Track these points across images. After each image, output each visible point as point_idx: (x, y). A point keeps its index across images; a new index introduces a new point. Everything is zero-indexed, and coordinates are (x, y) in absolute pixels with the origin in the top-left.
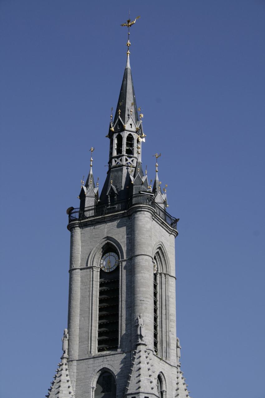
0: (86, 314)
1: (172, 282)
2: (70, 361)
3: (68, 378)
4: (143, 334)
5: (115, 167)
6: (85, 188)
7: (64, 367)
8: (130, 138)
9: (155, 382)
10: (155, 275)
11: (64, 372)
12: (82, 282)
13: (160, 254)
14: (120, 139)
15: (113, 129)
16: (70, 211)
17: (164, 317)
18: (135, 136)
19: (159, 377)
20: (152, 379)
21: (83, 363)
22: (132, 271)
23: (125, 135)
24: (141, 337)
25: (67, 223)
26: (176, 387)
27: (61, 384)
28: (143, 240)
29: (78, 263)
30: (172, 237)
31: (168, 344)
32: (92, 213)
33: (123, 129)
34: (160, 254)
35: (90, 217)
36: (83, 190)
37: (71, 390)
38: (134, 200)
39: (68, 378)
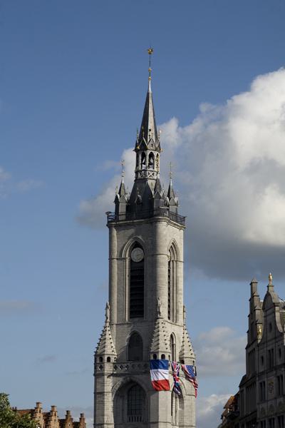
0: (121, 292)
1: (181, 266)
2: (111, 324)
3: (110, 337)
4: (161, 311)
5: (140, 179)
6: (118, 196)
7: (108, 329)
8: (151, 155)
9: (169, 338)
10: (169, 262)
11: (108, 333)
12: (118, 268)
13: (173, 248)
14: (144, 156)
15: (138, 148)
16: (108, 213)
17: (175, 292)
18: (155, 153)
19: (171, 336)
20: (166, 342)
21: (120, 327)
22: (154, 264)
23: (148, 153)
24: (160, 313)
25: (106, 223)
26: (182, 340)
27: (106, 341)
28: (161, 244)
29: (115, 254)
30: (182, 231)
31: (177, 311)
32: (124, 217)
33: (147, 149)
34: (173, 248)
35: (122, 221)
36: (117, 197)
37: (113, 345)
38: (155, 213)
39: (110, 337)
